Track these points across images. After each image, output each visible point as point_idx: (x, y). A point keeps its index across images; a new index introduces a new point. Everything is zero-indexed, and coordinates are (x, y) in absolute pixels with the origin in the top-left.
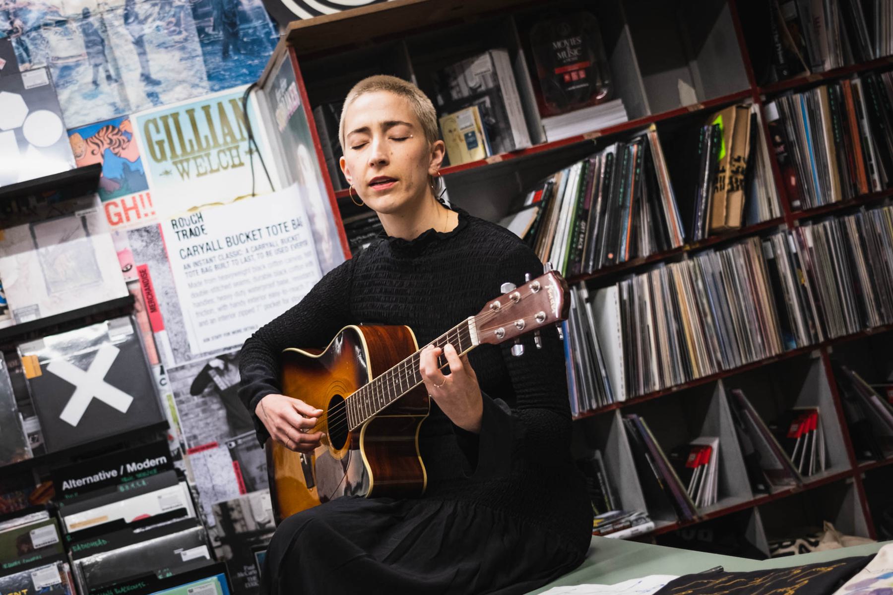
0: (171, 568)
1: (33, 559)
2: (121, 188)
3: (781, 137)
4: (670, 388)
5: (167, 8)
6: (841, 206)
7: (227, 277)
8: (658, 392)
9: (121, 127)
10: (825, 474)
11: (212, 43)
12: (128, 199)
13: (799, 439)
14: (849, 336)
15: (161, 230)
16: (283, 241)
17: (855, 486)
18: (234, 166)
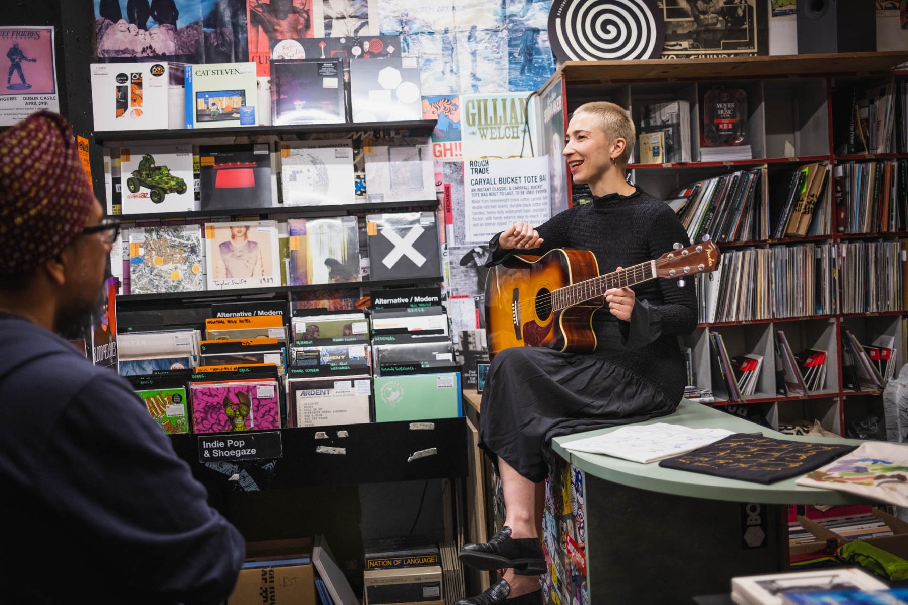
0: (429, 362)
1: (351, 340)
2: (446, 136)
3: (841, 187)
4: (741, 322)
5: (494, 37)
6: (868, 236)
7: (495, 201)
8: (734, 322)
9: (453, 101)
10: (822, 392)
11: (516, 63)
12: (448, 144)
13: (811, 368)
14: (855, 314)
15: (463, 166)
16: (532, 187)
17: (839, 402)
18: (513, 137)
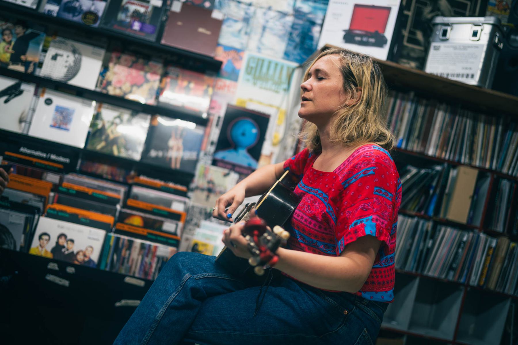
12: (228, 82)
